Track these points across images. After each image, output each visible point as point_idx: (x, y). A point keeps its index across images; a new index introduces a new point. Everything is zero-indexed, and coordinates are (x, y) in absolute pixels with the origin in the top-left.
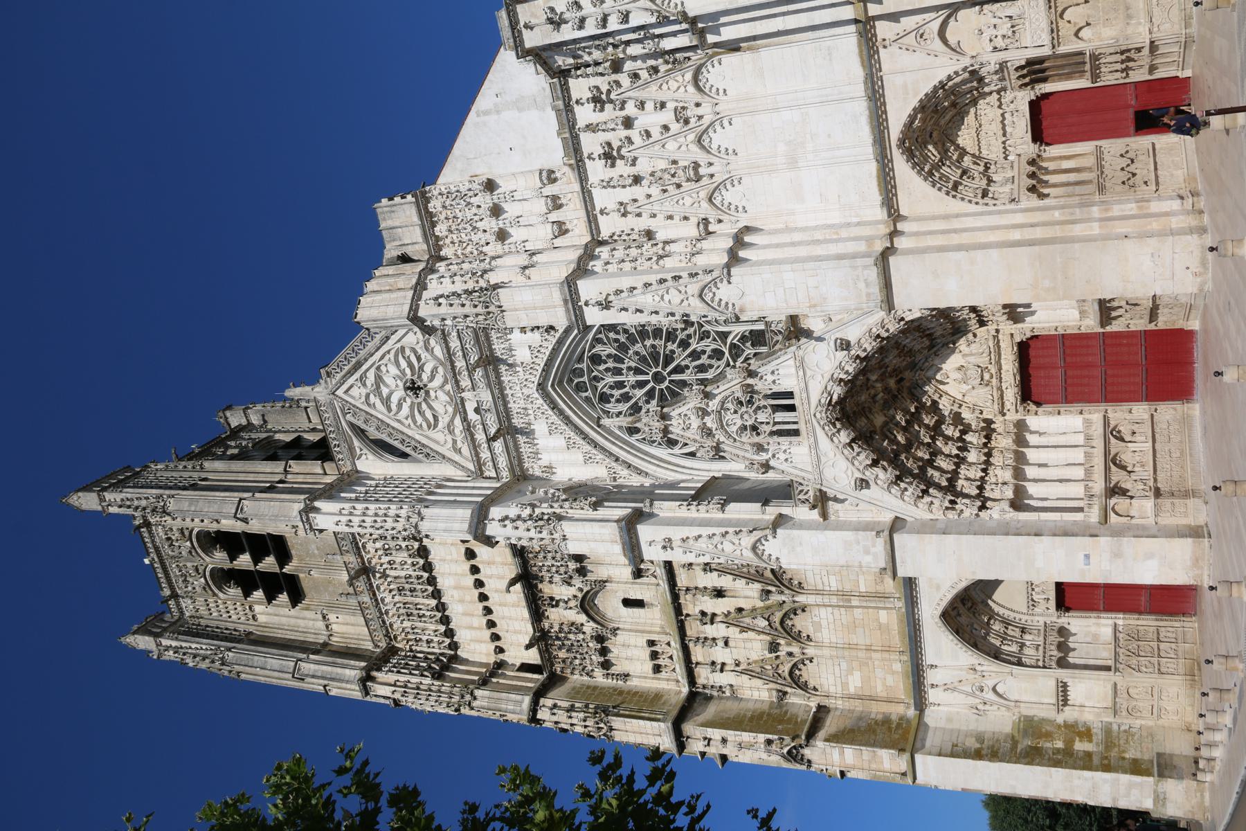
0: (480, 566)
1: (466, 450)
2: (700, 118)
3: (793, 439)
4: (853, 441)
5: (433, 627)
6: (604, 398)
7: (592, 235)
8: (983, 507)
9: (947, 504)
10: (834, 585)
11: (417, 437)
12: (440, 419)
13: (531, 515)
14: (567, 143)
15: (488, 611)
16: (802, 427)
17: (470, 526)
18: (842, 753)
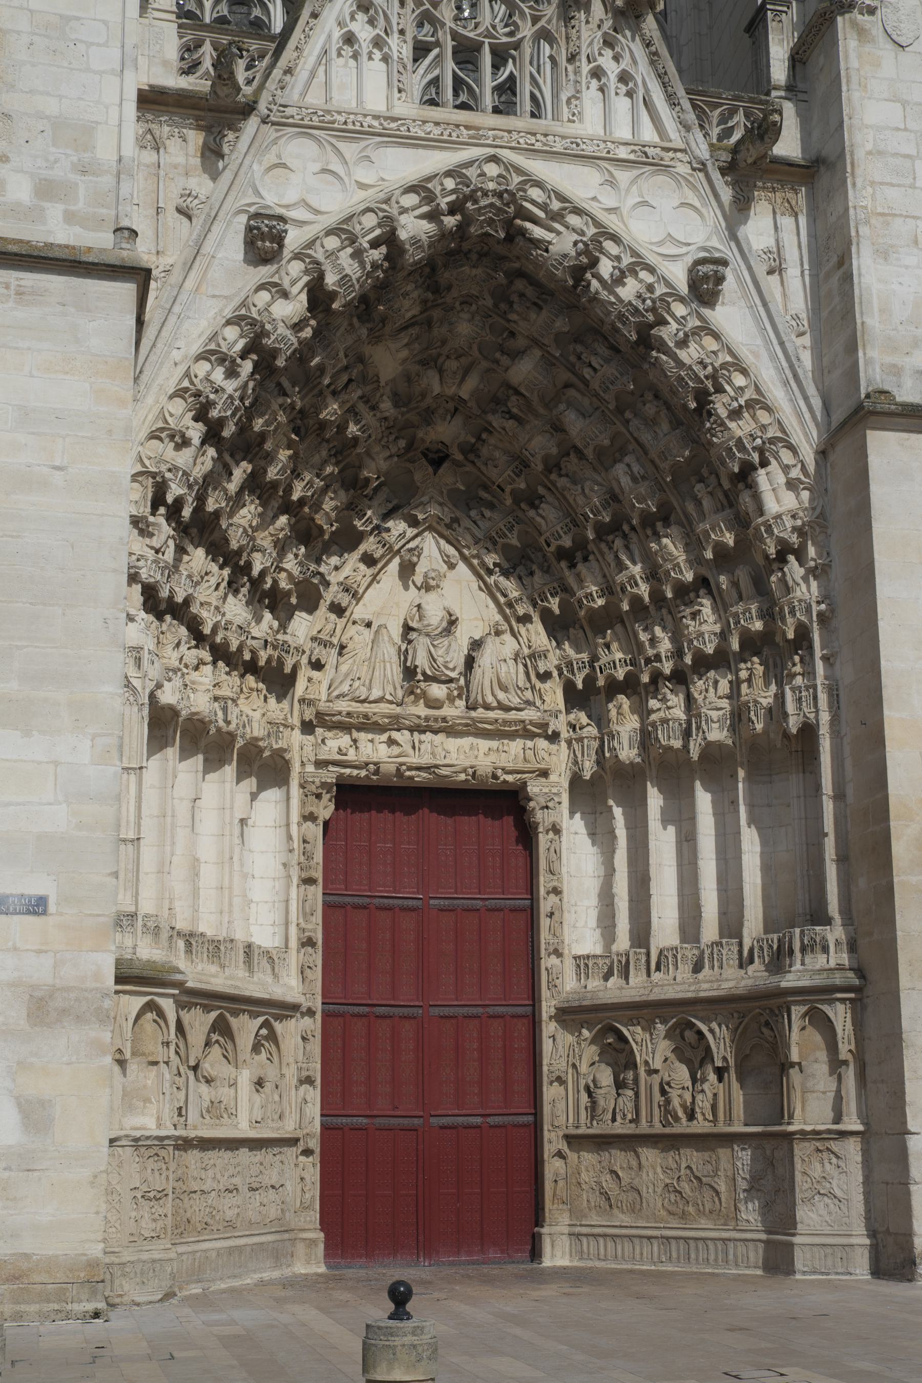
9: (175, 490)
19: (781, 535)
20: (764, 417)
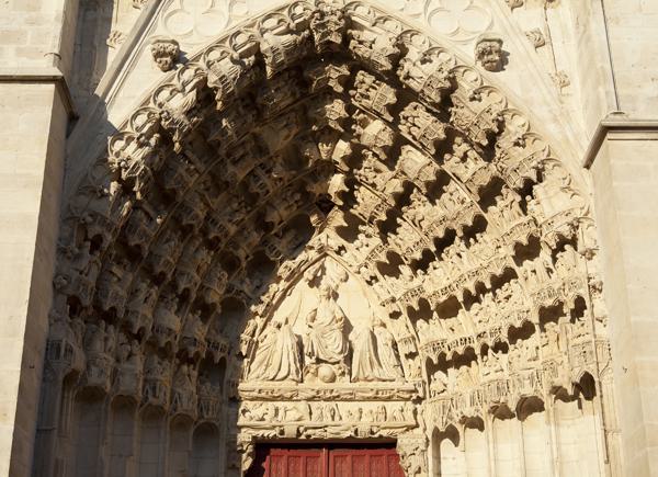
8: (75, 306)
9: (95, 230)
19: (559, 230)
20: (539, 145)
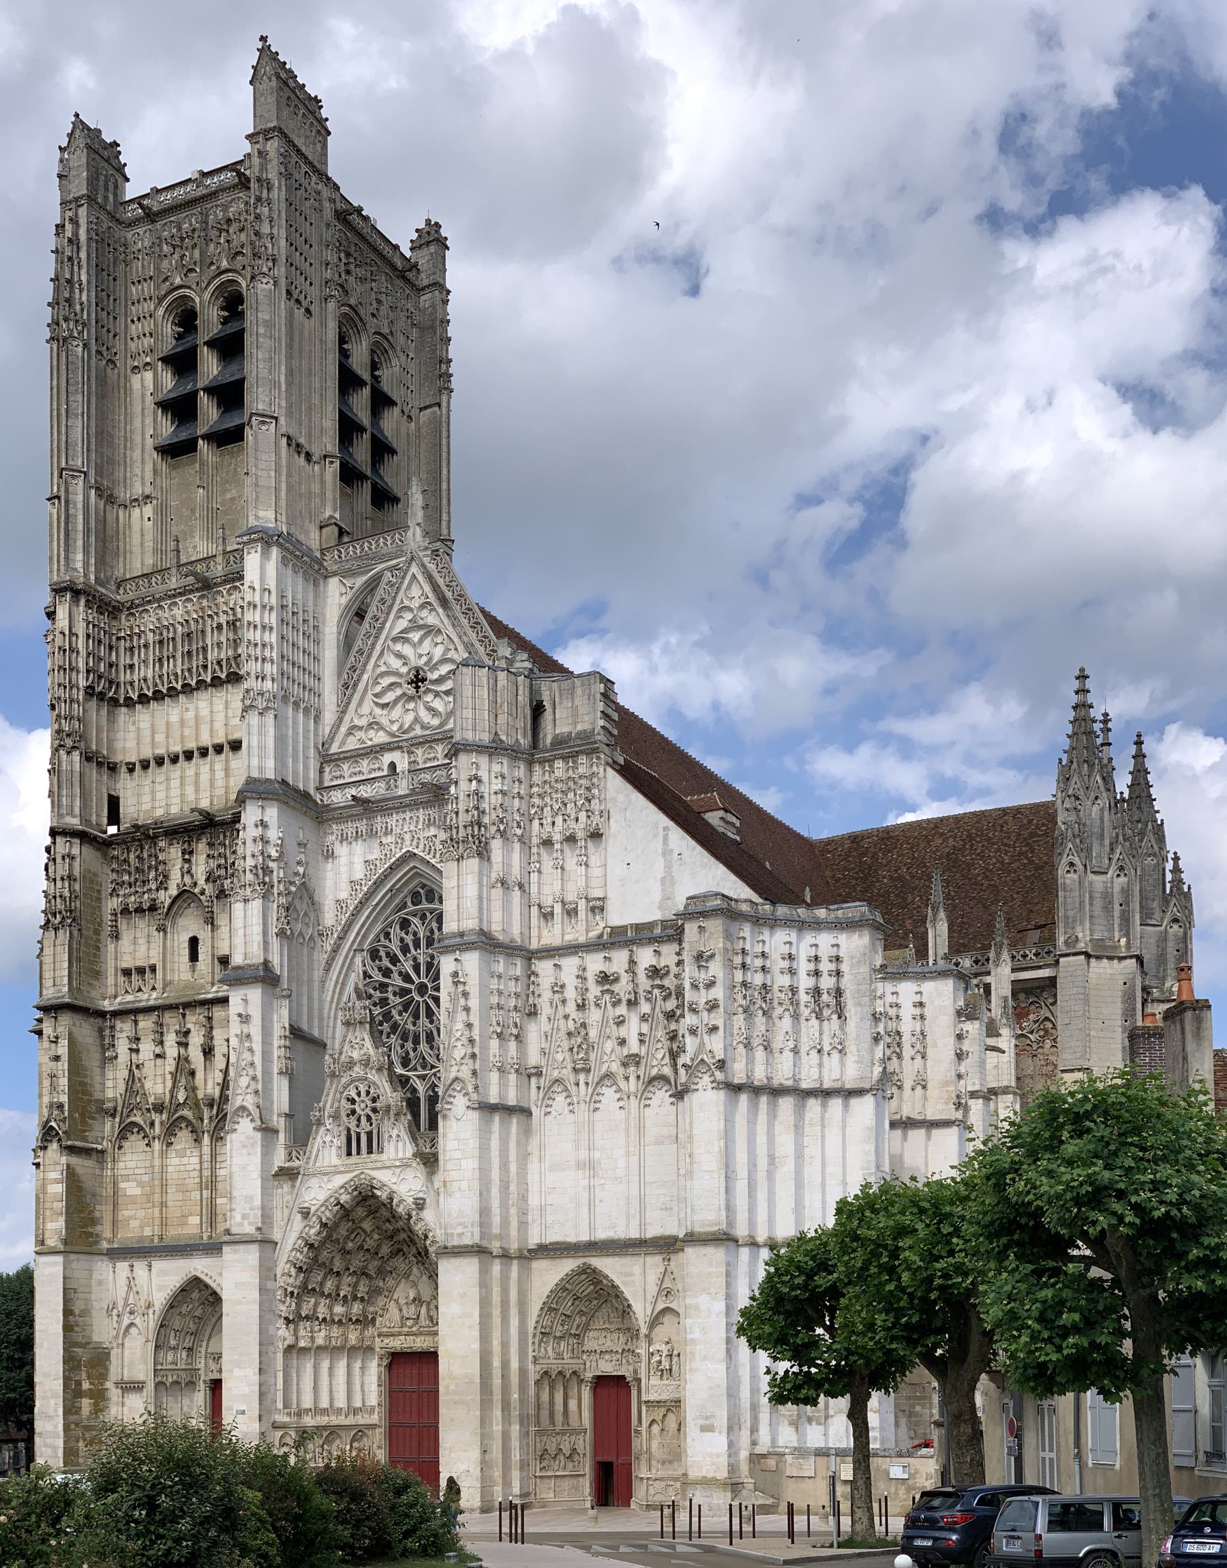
0: (223, 756)
1: (352, 744)
2: (627, 1078)
3: (344, 1149)
4: (342, 1206)
5: (150, 675)
6: (405, 924)
7: (538, 951)
8: (288, 1321)
9: (290, 1289)
10: (221, 1173)
11: (365, 677)
12: (385, 712)
13: (269, 856)
14: (619, 934)
15: (175, 759)
16: (354, 1159)
17: (255, 780)
18: (56, 1181)
